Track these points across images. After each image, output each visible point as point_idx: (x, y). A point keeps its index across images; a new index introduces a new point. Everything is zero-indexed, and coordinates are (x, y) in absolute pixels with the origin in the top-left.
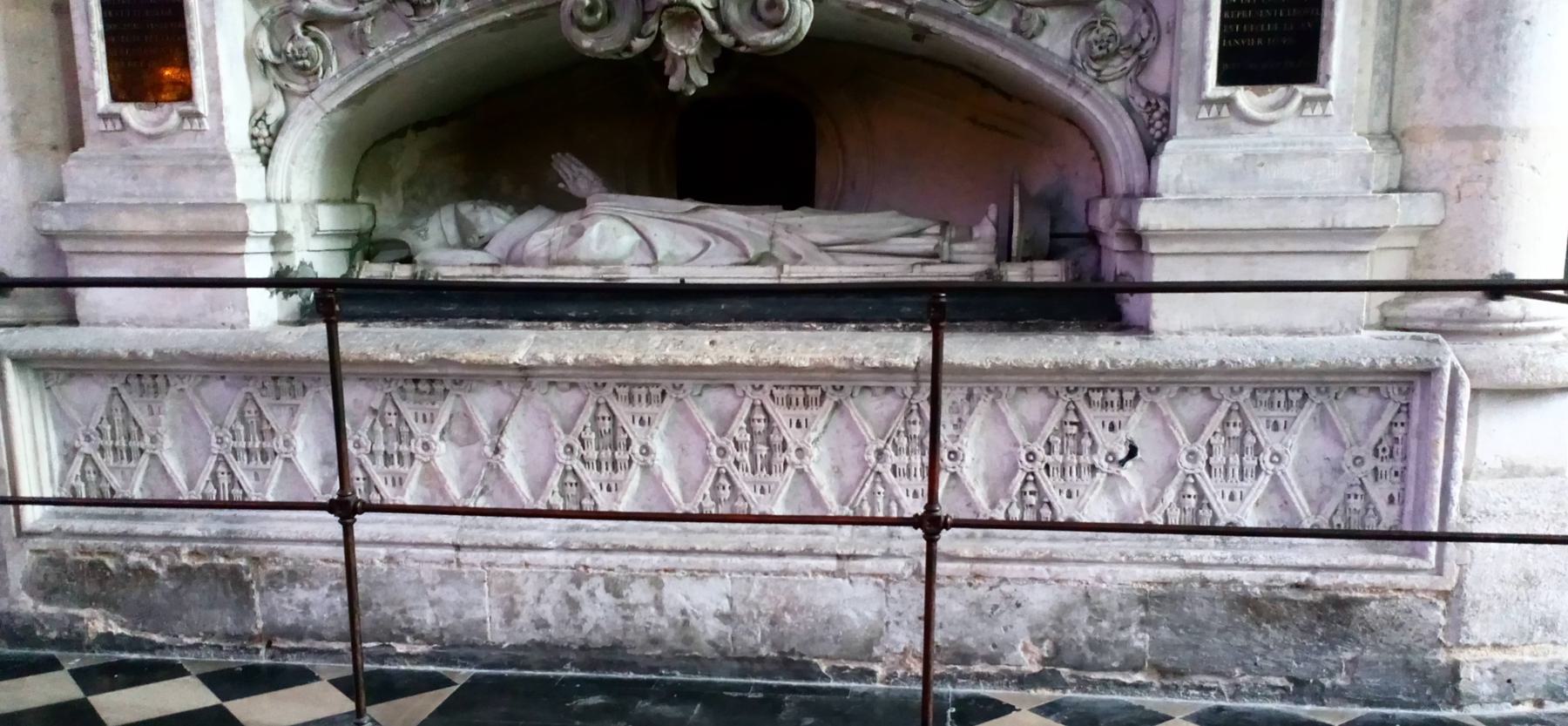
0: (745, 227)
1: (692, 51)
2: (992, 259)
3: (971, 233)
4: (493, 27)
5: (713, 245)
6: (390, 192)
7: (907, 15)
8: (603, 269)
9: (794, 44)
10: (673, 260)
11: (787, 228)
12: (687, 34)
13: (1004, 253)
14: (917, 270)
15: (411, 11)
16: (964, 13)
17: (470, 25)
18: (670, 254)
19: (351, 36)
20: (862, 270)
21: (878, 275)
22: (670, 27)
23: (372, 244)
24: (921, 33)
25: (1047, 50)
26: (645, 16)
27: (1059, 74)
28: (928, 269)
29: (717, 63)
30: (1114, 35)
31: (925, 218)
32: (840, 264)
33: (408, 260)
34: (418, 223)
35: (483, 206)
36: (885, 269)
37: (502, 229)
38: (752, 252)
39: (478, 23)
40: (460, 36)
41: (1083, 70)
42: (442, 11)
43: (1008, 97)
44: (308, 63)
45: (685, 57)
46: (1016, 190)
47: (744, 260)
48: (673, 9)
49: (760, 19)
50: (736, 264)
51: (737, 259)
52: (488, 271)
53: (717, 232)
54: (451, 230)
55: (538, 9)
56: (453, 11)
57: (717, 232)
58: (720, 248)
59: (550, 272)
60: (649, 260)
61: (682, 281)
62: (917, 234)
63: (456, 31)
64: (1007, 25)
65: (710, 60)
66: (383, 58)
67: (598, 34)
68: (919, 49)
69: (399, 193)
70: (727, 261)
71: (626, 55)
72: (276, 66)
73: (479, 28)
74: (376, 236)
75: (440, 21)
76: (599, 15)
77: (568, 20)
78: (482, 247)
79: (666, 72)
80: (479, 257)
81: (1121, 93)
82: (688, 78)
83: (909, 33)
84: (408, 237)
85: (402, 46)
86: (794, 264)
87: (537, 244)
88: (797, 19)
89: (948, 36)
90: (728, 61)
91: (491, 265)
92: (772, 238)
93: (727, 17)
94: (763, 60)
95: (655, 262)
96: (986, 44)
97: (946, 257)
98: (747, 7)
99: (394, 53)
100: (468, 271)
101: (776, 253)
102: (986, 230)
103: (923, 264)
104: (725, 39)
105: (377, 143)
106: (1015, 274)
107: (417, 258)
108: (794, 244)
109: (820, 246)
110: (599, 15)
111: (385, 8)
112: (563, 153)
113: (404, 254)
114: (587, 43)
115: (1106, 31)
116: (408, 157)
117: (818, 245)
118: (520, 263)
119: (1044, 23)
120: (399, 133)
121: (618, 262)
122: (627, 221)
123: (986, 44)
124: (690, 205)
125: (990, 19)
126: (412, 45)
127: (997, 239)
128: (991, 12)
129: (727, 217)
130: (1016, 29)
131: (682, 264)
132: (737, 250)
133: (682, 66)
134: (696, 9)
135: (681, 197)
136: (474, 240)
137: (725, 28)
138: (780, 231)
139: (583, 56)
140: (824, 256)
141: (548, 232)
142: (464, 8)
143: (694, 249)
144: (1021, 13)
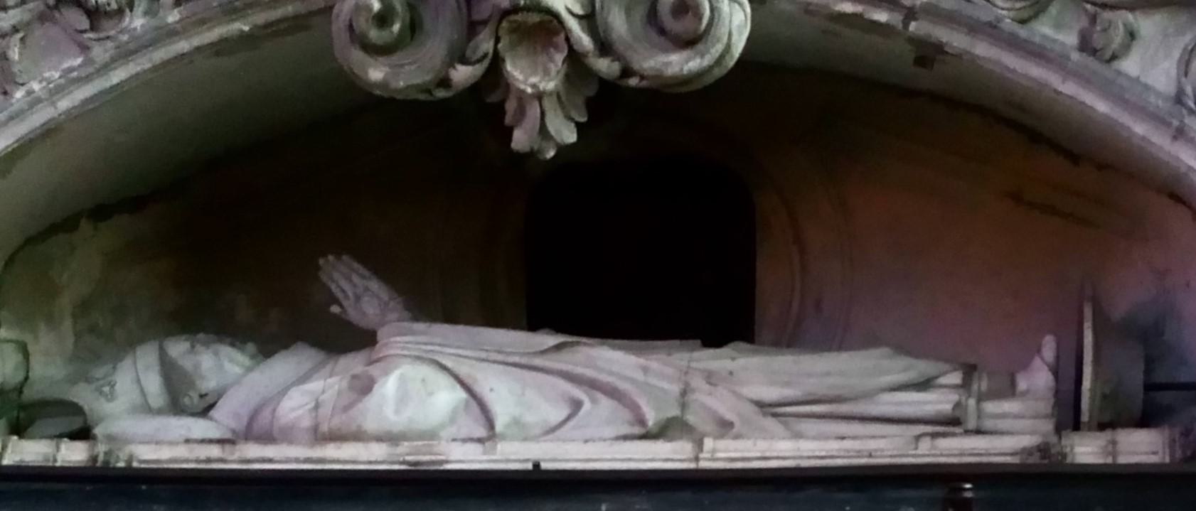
0: (639, 376)
1: (550, 85)
2: (1048, 426)
3: (1013, 384)
4: (220, 48)
5: (587, 405)
6: (52, 321)
7: (906, 25)
8: (404, 447)
9: (718, 73)
10: (521, 431)
11: (710, 378)
12: (542, 58)
13: (1068, 416)
14: (925, 445)
15: (84, 23)
16: (999, 20)
17: (183, 46)
18: (516, 422)
20: (834, 446)
21: (859, 454)
22: (512, 47)
23: (23, 407)
24: (929, 53)
25: (1137, 80)
26: (473, 28)
27: (1158, 119)
28: (945, 444)
29: (592, 106)
31: (938, 358)
32: (798, 436)
33: (83, 434)
34: (99, 372)
35: (206, 344)
36: (872, 445)
37: (237, 381)
38: (652, 418)
39: (197, 41)
40: (165, 64)
42: (137, 22)
43: (1074, 158)
45: (539, 96)
46: (1088, 312)
47: (637, 430)
48: (519, 17)
49: (662, 31)
50: (626, 438)
51: (626, 430)
52: (215, 451)
53: (592, 385)
54: (154, 384)
55: (296, 17)
56: (154, 22)
57: (592, 385)
58: (599, 411)
59: (318, 452)
60: (481, 432)
61: (537, 465)
62: (924, 385)
63: (161, 54)
64: (1070, 39)
65: (580, 101)
66: (39, 100)
67: (395, 58)
68: (925, 79)
69: (68, 324)
70: (610, 432)
71: (441, 94)
73: (198, 49)
74: (29, 394)
75: (134, 38)
76: (396, 27)
77: (345, 36)
78: (205, 411)
79: (508, 120)
80: (199, 428)
82: (543, 131)
83: (908, 53)
84: (82, 395)
85: (72, 81)
86: (721, 437)
87: (295, 407)
88: (722, 32)
89: (974, 59)
90: (610, 103)
91: (220, 442)
92: (684, 393)
93: (608, 28)
94: (667, 99)
95: (490, 435)
96: (1035, 71)
97: (972, 424)
98: (640, 12)
99: (57, 91)
100: (181, 452)
101: (691, 418)
102: (1038, 379)
103: (934, 436)
104: (604, 66)
105: (30, 241)
106: (1086, 450)
107: (98, 431)
108: (720, 403)
109: (764, 407)
110: (396, 27)
111: (42, 18)
112: (338, 256)
113: (76, 424)
114: (376, 73)
116: (82, 263)
117: (761, 405)
118: (267, 438)
119: (1132, 35)
120: (67, 225)
121: (430, 435)
122: (444, 368)
123: (1035, 71)
124: (548, 340)
125: (1043, 29)
126: (88, 79)
127: (1057, 393)
128: (1044, 18)
129: (611, 360)
130: (1085, 45)
131: (535, 438)
132: (626, 414)
133: (534, 111)
134: (556, 16)
135: (533, 327)
136: (192, 400)
137: (605, 47)
138: (698, 382)
139: (371, 94)
140: (770, 423)
141: (315, 385)
142: (173, 17)
143: (556, 413)
144: (1093, 19)
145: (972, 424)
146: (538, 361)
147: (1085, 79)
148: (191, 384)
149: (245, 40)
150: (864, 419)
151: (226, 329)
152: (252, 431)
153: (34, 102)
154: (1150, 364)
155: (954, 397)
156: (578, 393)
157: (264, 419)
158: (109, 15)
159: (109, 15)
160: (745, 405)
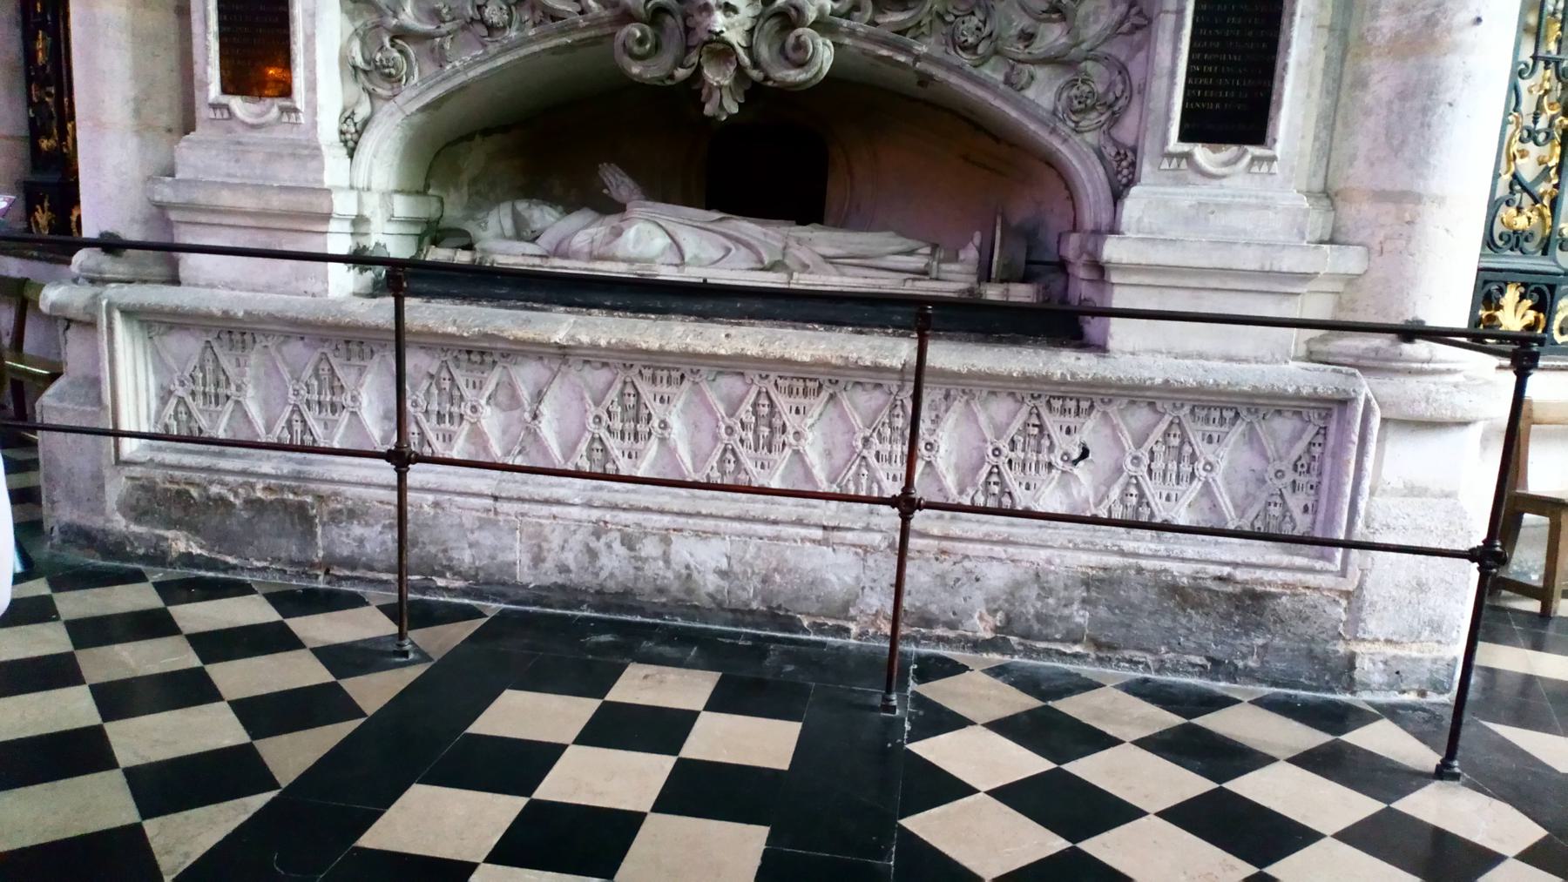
1: (726, 82)
2: (974, 279)
3: (957, 255)
4: (555, 51)
5: (734, 251)
6: (457, 187)
8: (637, 266)
9: (814, 82)
11: (799, 241)
13: (985, 275)
14: (909, 284)
15: (485, 33)
17: (536, 48)
18: (696, 257)
19: (432, 50)
20: (861, 281)
22: (708, 60)
23: (439, 231)
24: (925, 80)
26: (688, 50)
27: (1042, 122)
28: (919, 284)
29: (747, 94)
30: (1092, 92)
32: (843, 275)
33: (469, 247)
34: (480, 216)
36: (881, 282)
37: (552, 225)
38: (767, 260)
39: (543, 46)
41: (1064, 121)
42: (513, 33)
43: (997, 139)
44: (393, 71)
45: (720, 88)
46: (999, 221)
49: (787, 58)
51: (753, 265)
52: (537, 261)
53: (737, 241)
54: (508, 224)
57: (737, 241)
58: (740, 255)
59: (591, 265)
60: (677, 261)
62: (911, 253)
64: (1000, 77)
65: (741, 91)
67: (646, 62)
68: (923, 93)
70: (745, 266)
71: (669, 83)
72: (365, 72)
74: (442, 224)
77: (621, 49)
78: (534, 240)
80: (530, 248)
81: (1095, 143)
82: (721, 105)
84: (470, 227)
87: (581, 241)
90: (756, 93)
93: (758, 55)
95: (682, 263)
96: (981, 93)
97: (934, 275)
98: (776, 47)
99: (468, 67)
100: (520, 260)
101: (787, 261)
102: (971, 254)
104: (755, 74)
105: (448, 144)
106: (993, 293)
107: (477, 246)
108: (804, 255)
111: (463, 28)
113: (466, 242)
114: (635, 70)
115: (1086, 88)
116: (475, 158)
117: (825, 257)
118: (565, 256)
119: (1032, 78)
120: (469, 137)
121: (651, 261)
123: (981, 93)
124: (717, 215)
125: (986, 71)
126: (485, 62)
129: (747, 228)
130: (1007, 81)
132: (754, 257)
133: (717, 95)
134: (732, 46)
135: (708, 208)
136: (527, 233)
137: (756, 64)
138: (792, 243)
140: (829, 267)
141: (592, 230)
142: (532, 33)
143: (717, 254)
144: (1013, 68)
145: (934, 275)
146: (709, 226)
147: (1006, 99)
148: (528, 225)
149: (568, 46)
150: (878, 268)
151: (549, 198)
152: (558, 252)
153: (456, 72)
154: (1029, 250)
155: (926, 260)
156: (730, 244)
157: (564, 246)
158: (498, 29)
159: (498, 29)
160: (816, 257)
